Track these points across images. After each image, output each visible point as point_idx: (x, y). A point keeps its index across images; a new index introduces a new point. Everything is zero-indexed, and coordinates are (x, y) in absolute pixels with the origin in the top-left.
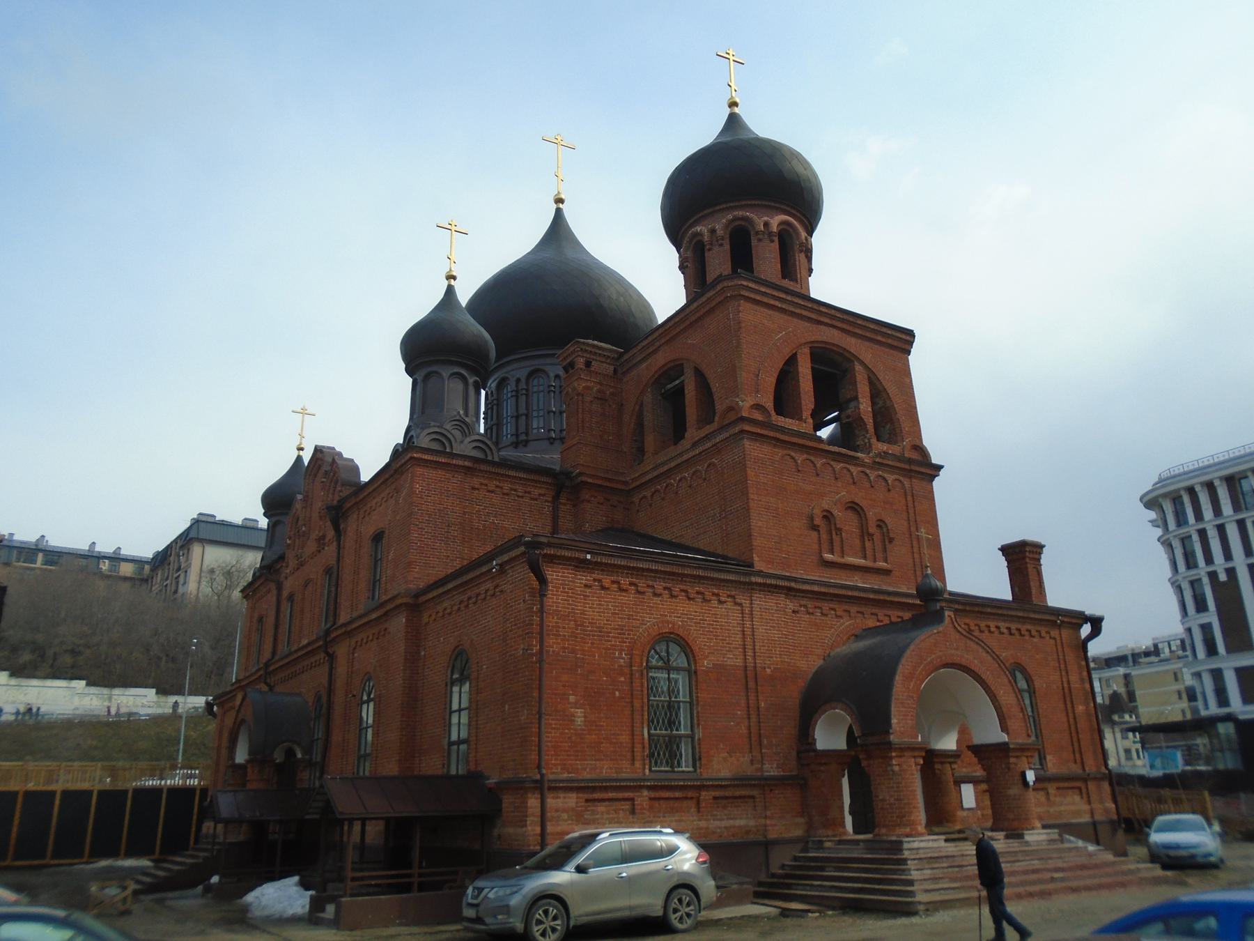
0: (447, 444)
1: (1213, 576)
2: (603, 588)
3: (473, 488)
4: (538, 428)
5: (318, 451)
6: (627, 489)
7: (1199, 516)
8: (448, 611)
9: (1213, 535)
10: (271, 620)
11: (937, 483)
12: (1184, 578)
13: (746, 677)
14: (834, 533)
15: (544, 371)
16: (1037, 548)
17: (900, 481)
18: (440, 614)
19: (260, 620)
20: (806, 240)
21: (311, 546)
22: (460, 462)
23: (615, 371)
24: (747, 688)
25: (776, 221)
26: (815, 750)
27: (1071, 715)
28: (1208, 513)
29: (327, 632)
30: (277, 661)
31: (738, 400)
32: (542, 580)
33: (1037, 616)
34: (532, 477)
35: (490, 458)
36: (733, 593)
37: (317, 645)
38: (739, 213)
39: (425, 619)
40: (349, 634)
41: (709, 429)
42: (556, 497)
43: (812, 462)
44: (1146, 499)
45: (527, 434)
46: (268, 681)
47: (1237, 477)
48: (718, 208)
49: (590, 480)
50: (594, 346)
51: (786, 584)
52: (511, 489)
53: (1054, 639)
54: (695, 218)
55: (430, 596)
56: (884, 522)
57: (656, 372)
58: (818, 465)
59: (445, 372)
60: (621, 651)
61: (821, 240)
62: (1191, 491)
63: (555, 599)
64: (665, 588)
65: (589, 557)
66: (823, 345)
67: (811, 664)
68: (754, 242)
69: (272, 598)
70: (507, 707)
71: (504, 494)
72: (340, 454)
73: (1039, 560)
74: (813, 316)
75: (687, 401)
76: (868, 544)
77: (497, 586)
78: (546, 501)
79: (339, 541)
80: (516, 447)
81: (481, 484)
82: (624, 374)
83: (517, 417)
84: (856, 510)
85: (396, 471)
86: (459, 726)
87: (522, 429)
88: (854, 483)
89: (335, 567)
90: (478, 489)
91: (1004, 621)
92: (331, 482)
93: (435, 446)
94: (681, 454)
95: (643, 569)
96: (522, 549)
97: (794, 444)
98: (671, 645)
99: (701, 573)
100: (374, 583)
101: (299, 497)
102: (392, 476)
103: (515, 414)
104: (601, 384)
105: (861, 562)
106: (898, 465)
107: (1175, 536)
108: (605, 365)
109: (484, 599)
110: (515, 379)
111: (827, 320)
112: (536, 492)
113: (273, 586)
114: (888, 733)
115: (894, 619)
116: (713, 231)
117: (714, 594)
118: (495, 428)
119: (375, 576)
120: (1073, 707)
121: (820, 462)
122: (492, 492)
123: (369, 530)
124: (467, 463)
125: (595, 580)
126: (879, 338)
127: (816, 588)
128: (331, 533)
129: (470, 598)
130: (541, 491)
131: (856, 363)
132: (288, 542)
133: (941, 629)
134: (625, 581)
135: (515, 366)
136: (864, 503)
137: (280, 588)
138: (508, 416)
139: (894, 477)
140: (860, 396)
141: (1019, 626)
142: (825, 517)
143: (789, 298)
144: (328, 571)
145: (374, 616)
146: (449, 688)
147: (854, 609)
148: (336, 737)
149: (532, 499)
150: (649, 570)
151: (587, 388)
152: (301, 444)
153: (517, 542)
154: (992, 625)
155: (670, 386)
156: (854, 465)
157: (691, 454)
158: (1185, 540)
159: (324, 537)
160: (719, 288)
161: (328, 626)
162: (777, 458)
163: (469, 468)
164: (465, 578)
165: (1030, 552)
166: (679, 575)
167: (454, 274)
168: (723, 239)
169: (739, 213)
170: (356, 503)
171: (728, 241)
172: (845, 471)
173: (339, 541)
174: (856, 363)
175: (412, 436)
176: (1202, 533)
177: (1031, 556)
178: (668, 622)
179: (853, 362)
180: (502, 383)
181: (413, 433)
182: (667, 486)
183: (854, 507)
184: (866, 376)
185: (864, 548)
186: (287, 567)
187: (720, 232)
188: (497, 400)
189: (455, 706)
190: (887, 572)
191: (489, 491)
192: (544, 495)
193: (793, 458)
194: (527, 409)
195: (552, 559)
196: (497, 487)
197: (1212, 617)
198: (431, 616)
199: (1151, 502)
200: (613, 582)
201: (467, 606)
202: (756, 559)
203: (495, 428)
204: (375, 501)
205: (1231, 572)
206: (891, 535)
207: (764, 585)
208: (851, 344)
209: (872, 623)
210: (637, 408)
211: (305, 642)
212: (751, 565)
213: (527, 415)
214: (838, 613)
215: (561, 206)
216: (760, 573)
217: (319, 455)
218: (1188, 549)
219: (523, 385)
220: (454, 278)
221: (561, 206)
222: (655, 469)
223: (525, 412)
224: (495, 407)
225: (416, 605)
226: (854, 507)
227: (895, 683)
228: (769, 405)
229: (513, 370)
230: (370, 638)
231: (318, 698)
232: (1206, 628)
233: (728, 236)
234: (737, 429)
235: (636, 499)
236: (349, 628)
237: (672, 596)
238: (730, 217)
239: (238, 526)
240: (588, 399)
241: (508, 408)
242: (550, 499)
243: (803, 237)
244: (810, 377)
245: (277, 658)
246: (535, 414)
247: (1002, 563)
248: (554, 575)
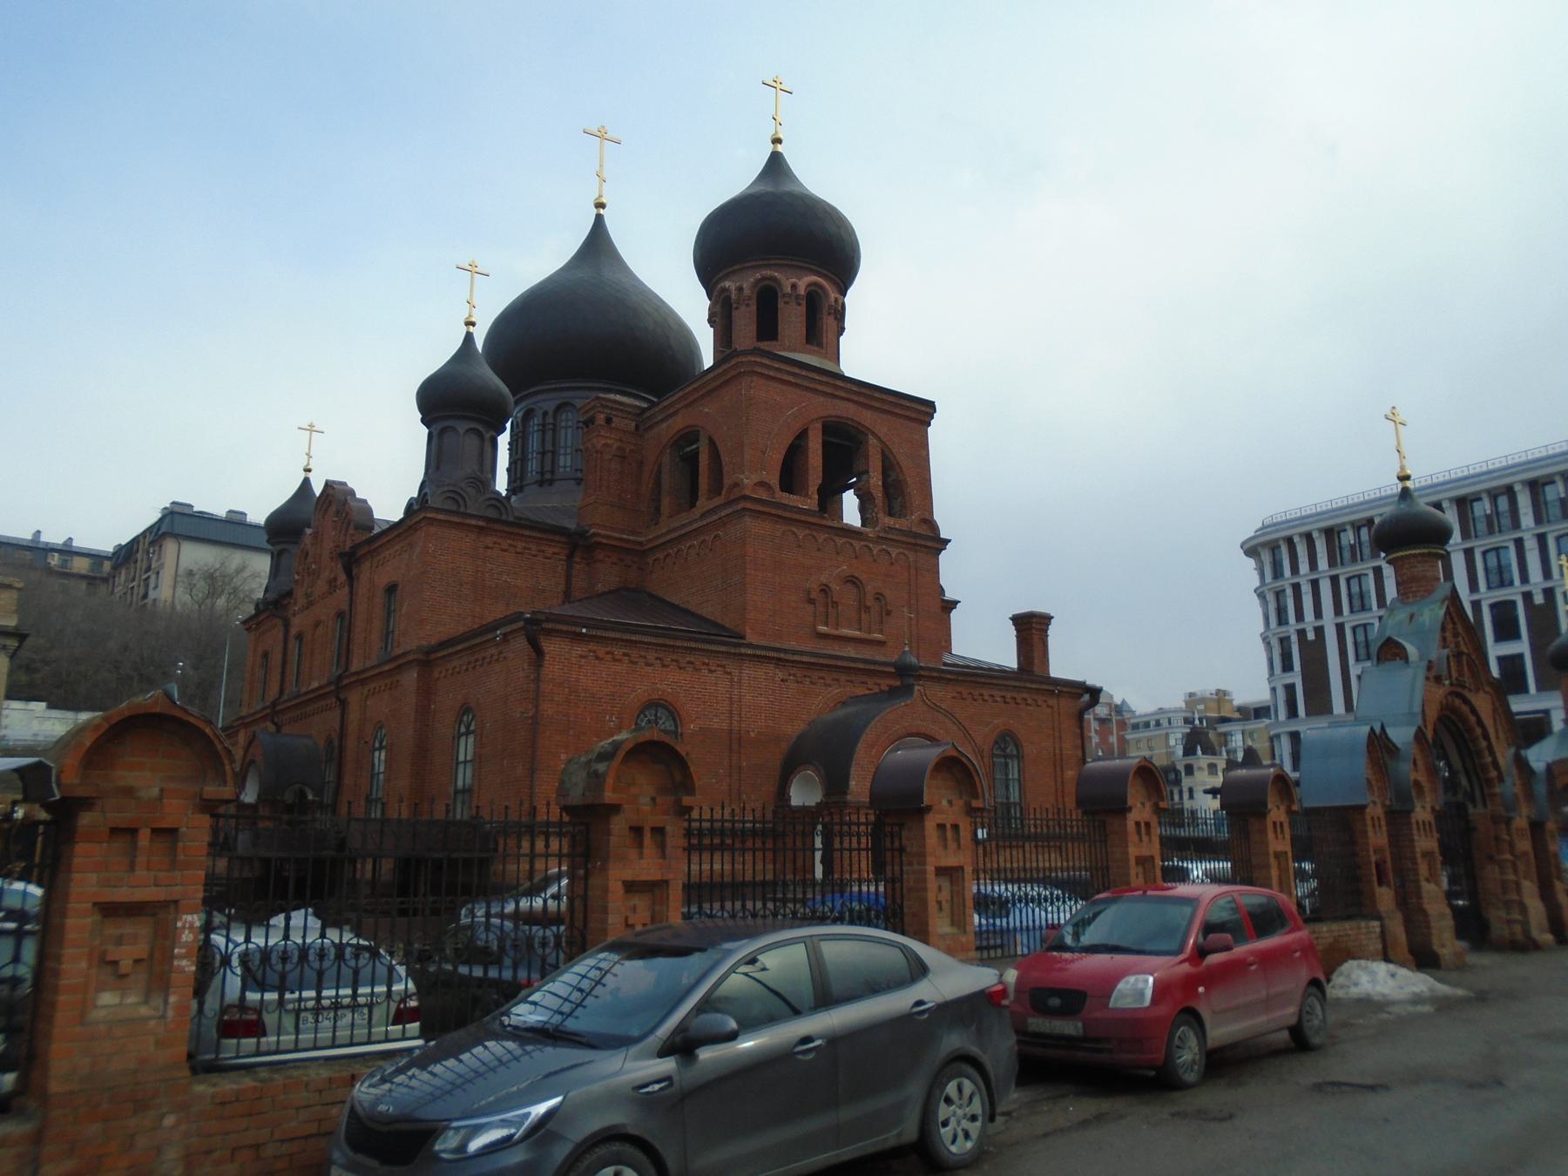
0: (461, 502)
1: (1302, 633)
2: (597, 658)
3: (487, 547)
4: (565, 467)
5: (329, 485)
6: (642, 549)
7: (1295, 570)
8: (457, 670)
9: (1306, 589)
10: (277, 657)
11: (943, 557)
12: (1274, 635)
13: (731, 740)
14: (830, 605)
15: (572, 405)
16: (1045, 620)
17: (905, 555)
18: (450, 672)
19: (265, 655)
20: (836, 300)
21: (321, 586)
22: (473, 522)
23: (637, 427)
24: (731, 749)
25: (804, 282)
26: (789, 806)
27: (1059, 780)
28: (1304, 567)
29: (340, 678)
30: (285, 701)
31: (742, 476)
32: (539, 652)
33: (1034, 686)
34: (544, 536)
35: (504, 517)
36: (724, 663)
37: (327, 690)
38: (768, 273)
39: (436, 674)
40: (363, 682)
41: (717, 501)
42: (570, 556)
43: (814, 537)
44: (1246, 547)
45: (552, 472)
46: (276, 720)
47: (1336, 529)
48: (747, 265)
49: (605, 541)
50: (615, 402)
51: (775, 655)
52: (525, 548)
53: (1052, 707)
54: (725, 272)
55: (440, 654)
56: (882, 595)
57: (675, 434)
58: (820, 541)
59: (462, 426)
60: (612, 715)
61: (855, 299)
62: (1290, 541)
63: (552, 669)
64: (657, 658)
65: (584, 630)
67: (793, 729)
68: (781, 305)
69: (278, 633)
70: (505, 762)
71: (517, 553)
72: (352, 493)
73: (1046, 631)
74: (829, 390)
75: (700, 469)
76: (864, 616)
77: (501, 653)
78: (560, 560)
79: (351, 587)
80: (541, 486)
81: (495, 543)
82: (646, 430)
83: (543, 454)
84: (854, 583)
85: (411, 527)
86: (464, 777)
87: (548, 467)
88: (856, 557)
89: (348, 612)
90: (492, 548)
91: (1000, 690)
92: (343, 523)
93: (451, 506)
94: (690, 523)
95: (636, 642)
96: (521, 624)
97: (797, 521)
98: (660, 710)
99: (693, 645)
100: (387, 635)
101: (309, 531)
102: (405, 531)
103: (541, 450)
104: (621, 441)
105: (857, 633)
106: (904, 539)
107: (1269, 590)
108: (627, 421)
109: (490, 663)
110: (541, 412)
111: (843, 394)
112: (550, 551)
113: (279, 622)
114: (845, 793)
115: (884, 688)
116: (740, 289)
117: (704, 664)
118: (519, 462)
119: (388, 626)
120: (1062, 771)
122: (505, 551)
123: (383, 579)
124: (481, 523)
125: (590, 651)
126: (897, 411)
127: (805, 659)
128: (342, 577)
129: (477, 660)
130: (555, 550)
131: (870, 436)
132: (297, 577)
133: (909, 702)
134: (618, 652)
135: (540, 397)
136: (863, 577)
137: (287, 626)
138: (533, 451)
139: (898, 551)
140: (871, 470)
141: (1015, 695)
142: (823, 590)
143: (804, 373)
144: (340, 615)
145: (386, 668)
146: (456, 741)
147: (843, 678)
148: (348, 780)
149: (546, 558)
150: (641, 642)
151: (606, 445)
152: (308, 464)
153: (518, 616)
154: (986, 693)
155: (688, 449)
156: (858, 539)
157: (700, 524)
158: (1279, 594)
159: (335, 579)
160: (733, 362)
161: (340, 672)
162: (778, 534)
163: (481, 529)
164: (473, 642)
165: (1037, 623)
166: (671, 646)
167: (473, 320)
168: (750, 298)
169: (768, 273)
170: (369, 552)
171: (755, 301)
172: (848, 546)
173: (351, 587)
174: (870, 436)
175: (426, 494)
176: (1296, 588)
177: (1038, 627)
178: (658, 690)
179: (867, 435)
180: (528, 414)
181: (426, 490)
182: (678, 551)
183: (852, 581)
184: (879, 449)
185: (860, 621)
186: (295, 603)
187: (747, 292)
188: (523, 432)
189: (461, 758)
190: (881, 643)
191: (502, 550)
192: (557, 554)
193: (794, 533)
194: (554, 444)
195: (549, 632)
196: (510, 545)
197: (1296, 678)
198: (441, 672)
199: (1251, 550)
200: (608, 653)
201: (474, 668)
202: (748, 631)
203: (519, 462)
204: (387, 552)
205: (1319, 631)
206: (889, 608)
207: (754, 656)
208: (866, 418)
209: (861, 691)
210: (656, 467)
211: (315, 684)
212: (743, 637)
213: (553, 452)
214: (828, 682)
215: (602, 211)
216: (750, 646)
217: (331, 492)
218: (1282, 604)
219: (550, 420)
220: (473, 324)
221: (602, 211)
222: (669, 532)
223: (551, 448)
224: (520, 440)
225: (427, 660)
226: (852, 581)
227: (857, 750)
228: (774, 481)
229: (544, 400)
230: (383, 688)
231: (329, 742)
232: (1290, 689)
233: (755, 297)
234: (740, 507)
235: (650, 561)
236: (362, 677)
237: (664, 666)
238: (758, 276)
239: (221, 520)
240: (608, 457)
241: (534, 442)
242: (565, 558)
243: (833, 300)
244: (820, 452)
245: (285, 697)
246: (562, 451)
247: (1011, 632)
248: (551, 647)
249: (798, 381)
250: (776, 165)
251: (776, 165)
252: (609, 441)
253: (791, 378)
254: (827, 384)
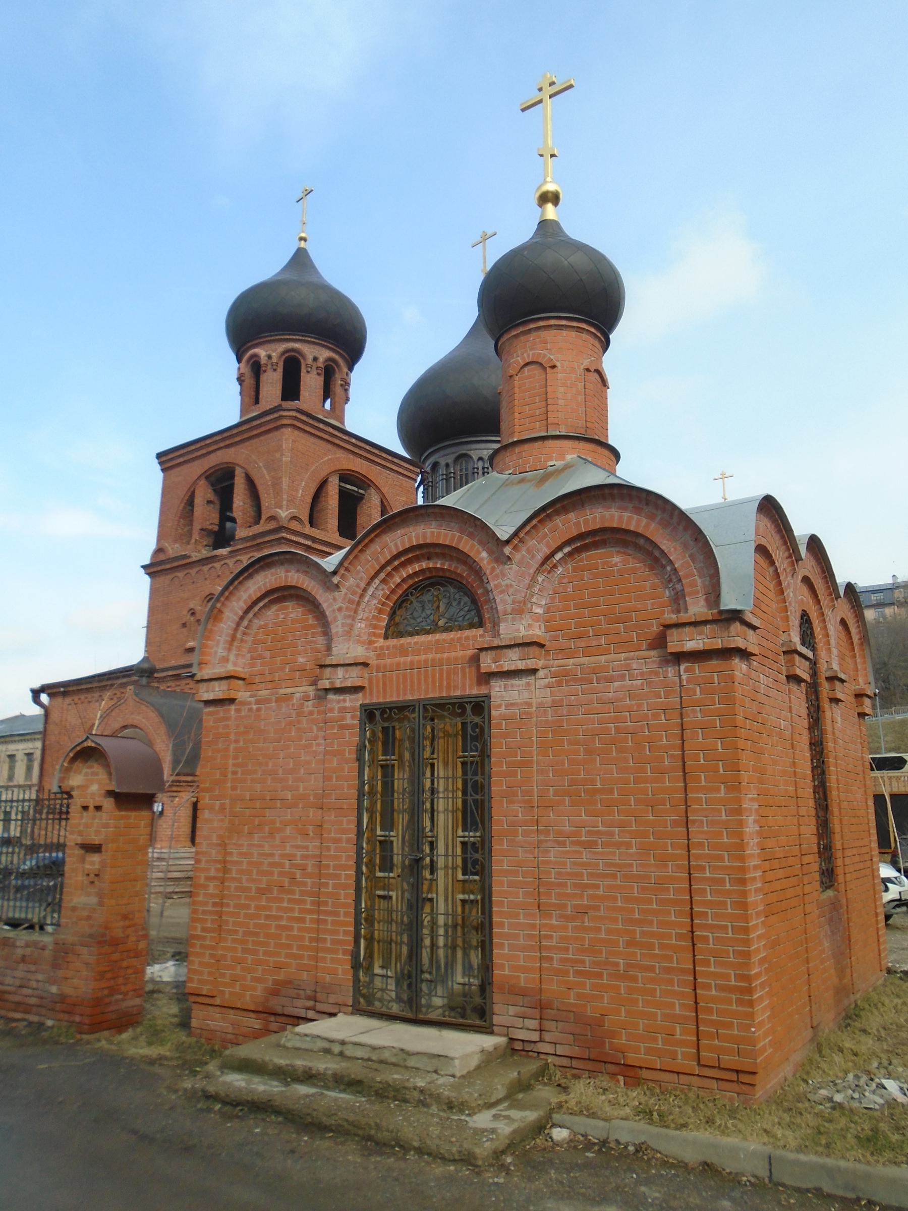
20: (269, 357)
66: (225, 466)
74: (204, 451)
106: (248, 544)
121: (193, 571)
126: (255, 432)
249: (186, 458)
250: (301, 259)
251: (301, 259)
253: (181, 460)
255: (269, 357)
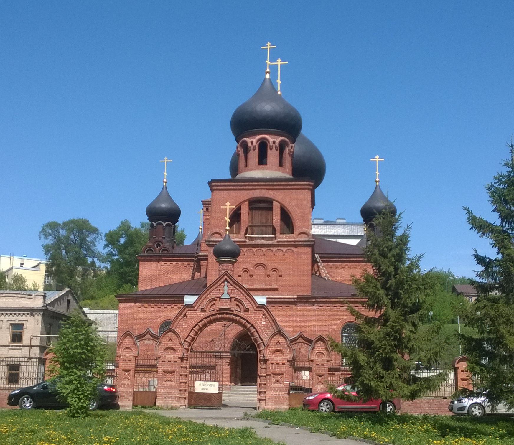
20: (274, 142)
74: (250, 187)
88: (264, 255)
149: (185, 266)
208: (270, 194)
249: (235, 188)
252: (208, 217)
254: (249, 185)
255: (274, 142)
